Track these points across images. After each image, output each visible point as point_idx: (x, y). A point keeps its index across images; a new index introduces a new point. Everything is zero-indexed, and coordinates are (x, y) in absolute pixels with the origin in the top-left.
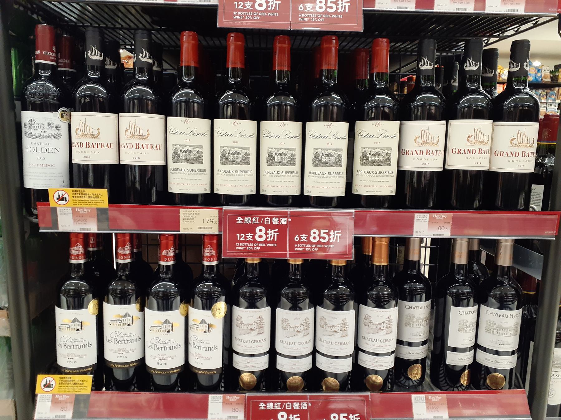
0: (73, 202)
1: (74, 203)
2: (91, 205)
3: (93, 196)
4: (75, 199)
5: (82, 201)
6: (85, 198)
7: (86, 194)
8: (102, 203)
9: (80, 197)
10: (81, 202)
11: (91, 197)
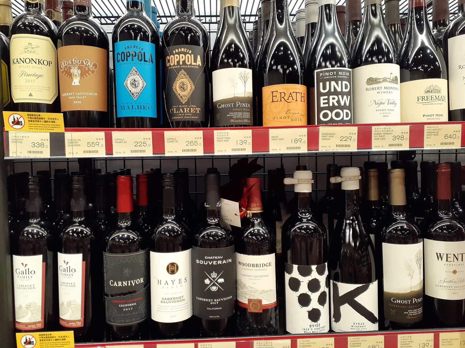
0: (29, 126)
2: (47, 129)
3: (49, 120)
4: (30, 123)
5: (38, 126)
6: (41, 122)
7: (42, 118)
8: (58, 127)
10: (37, 127)
11: (47, 122)
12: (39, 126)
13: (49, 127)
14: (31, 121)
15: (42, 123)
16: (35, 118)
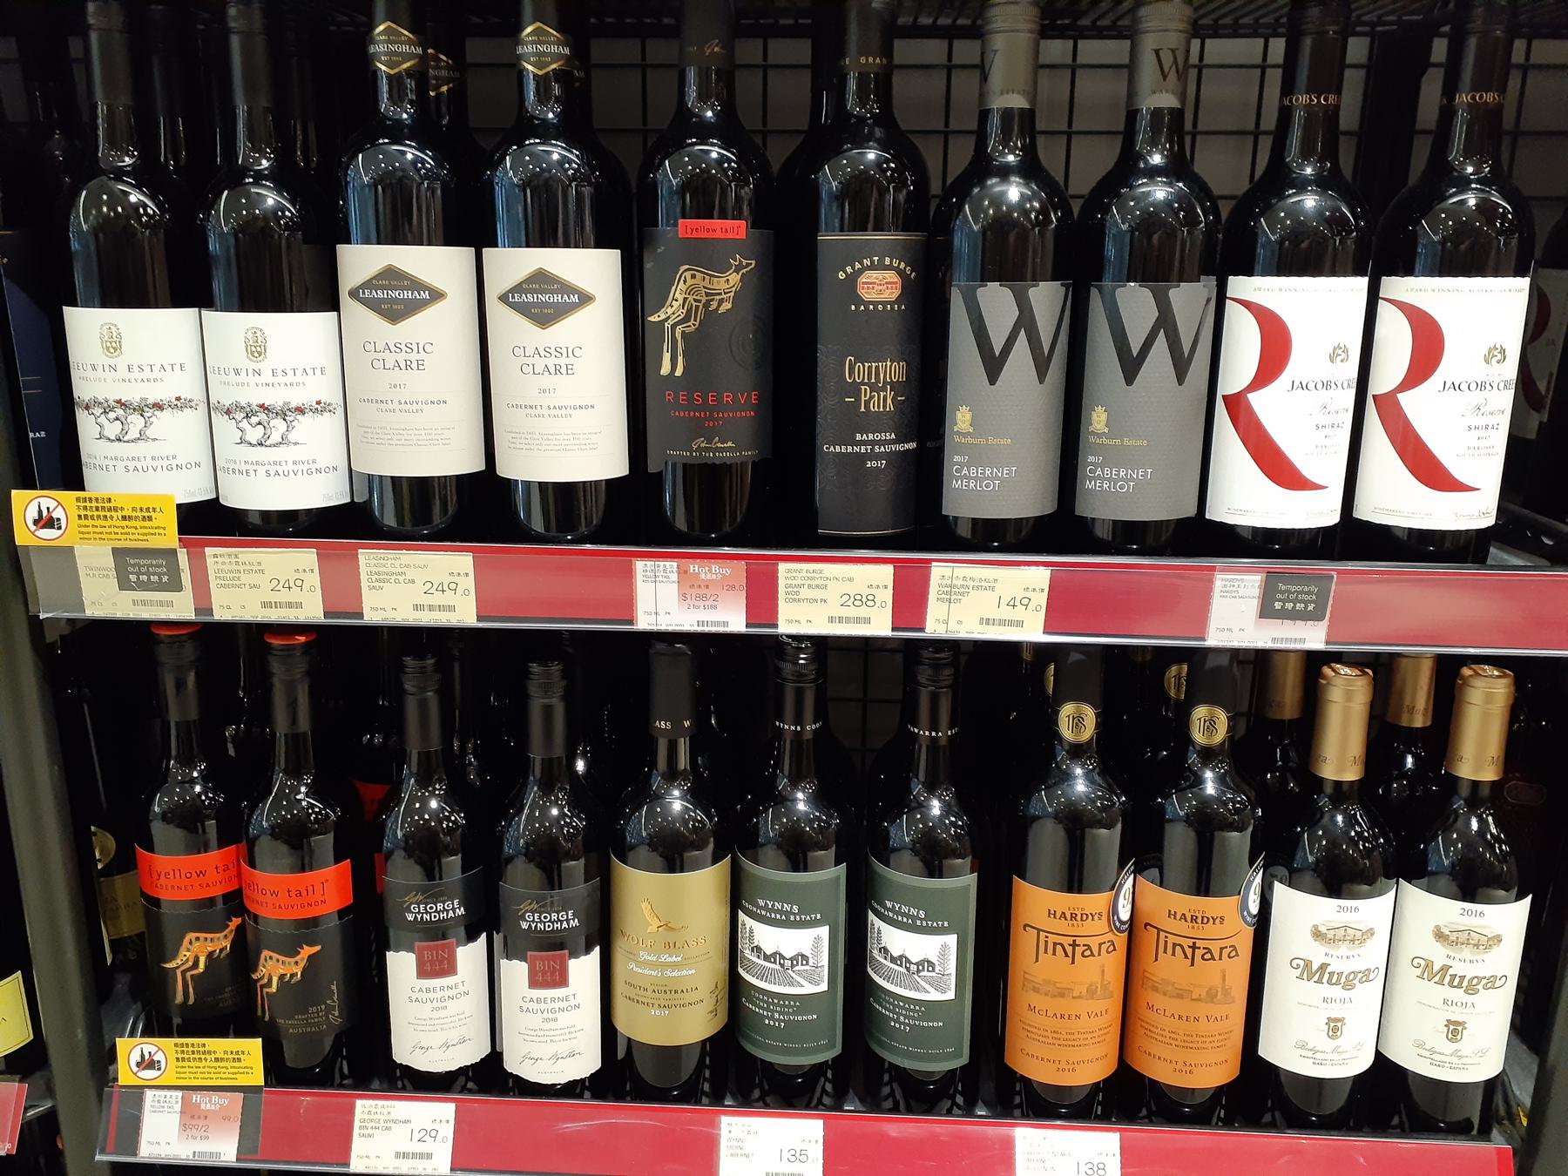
1: (178, 1075)
3: (226, 1056)
4: (180, 1064)
5: (199, 1070)
9: (194, 1059)
12: (202, 1070)
13: (225, 1073)
14: (183, 1059)
15: (208, 1064)
16: (193, 1052)
